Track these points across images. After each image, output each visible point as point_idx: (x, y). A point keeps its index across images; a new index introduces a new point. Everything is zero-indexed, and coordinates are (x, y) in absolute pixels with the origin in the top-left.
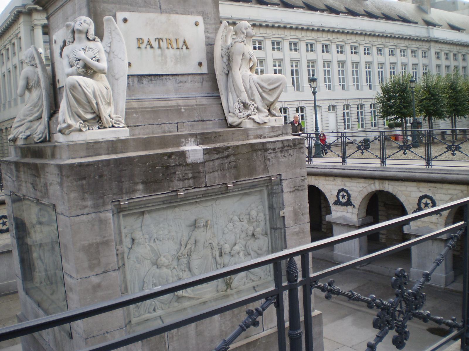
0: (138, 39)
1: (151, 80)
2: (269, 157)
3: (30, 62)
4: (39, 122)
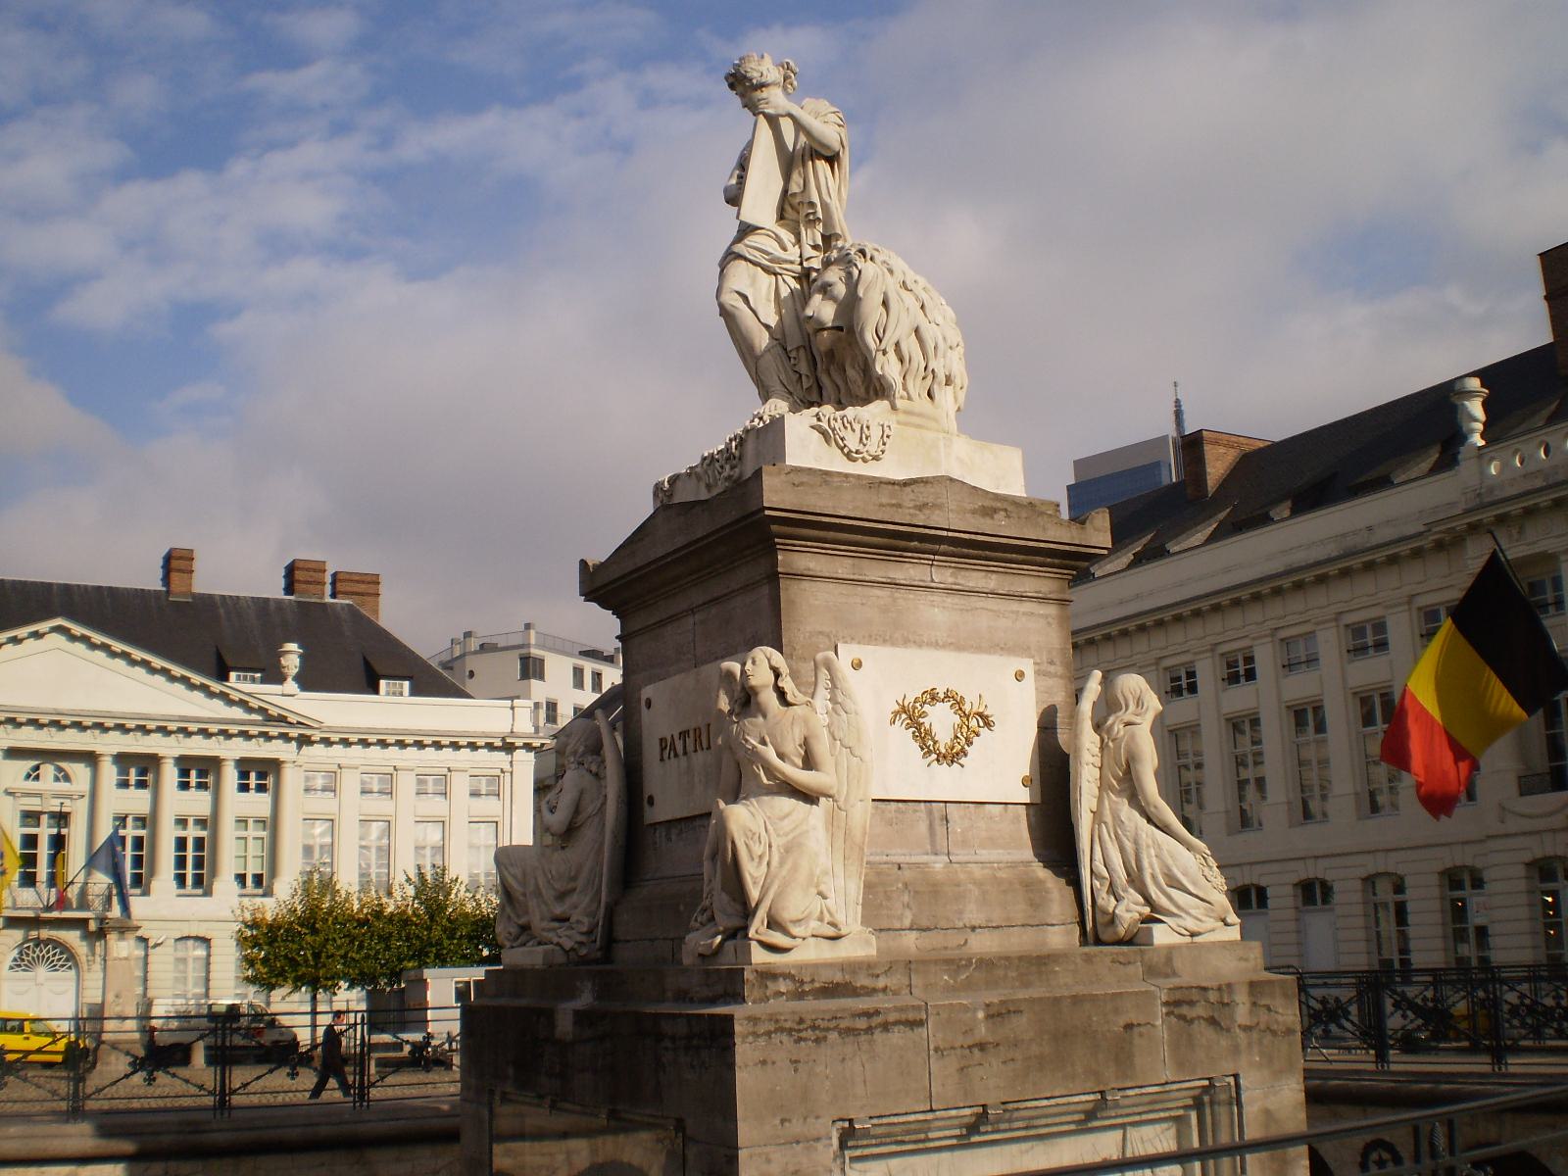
0: (661, 740)
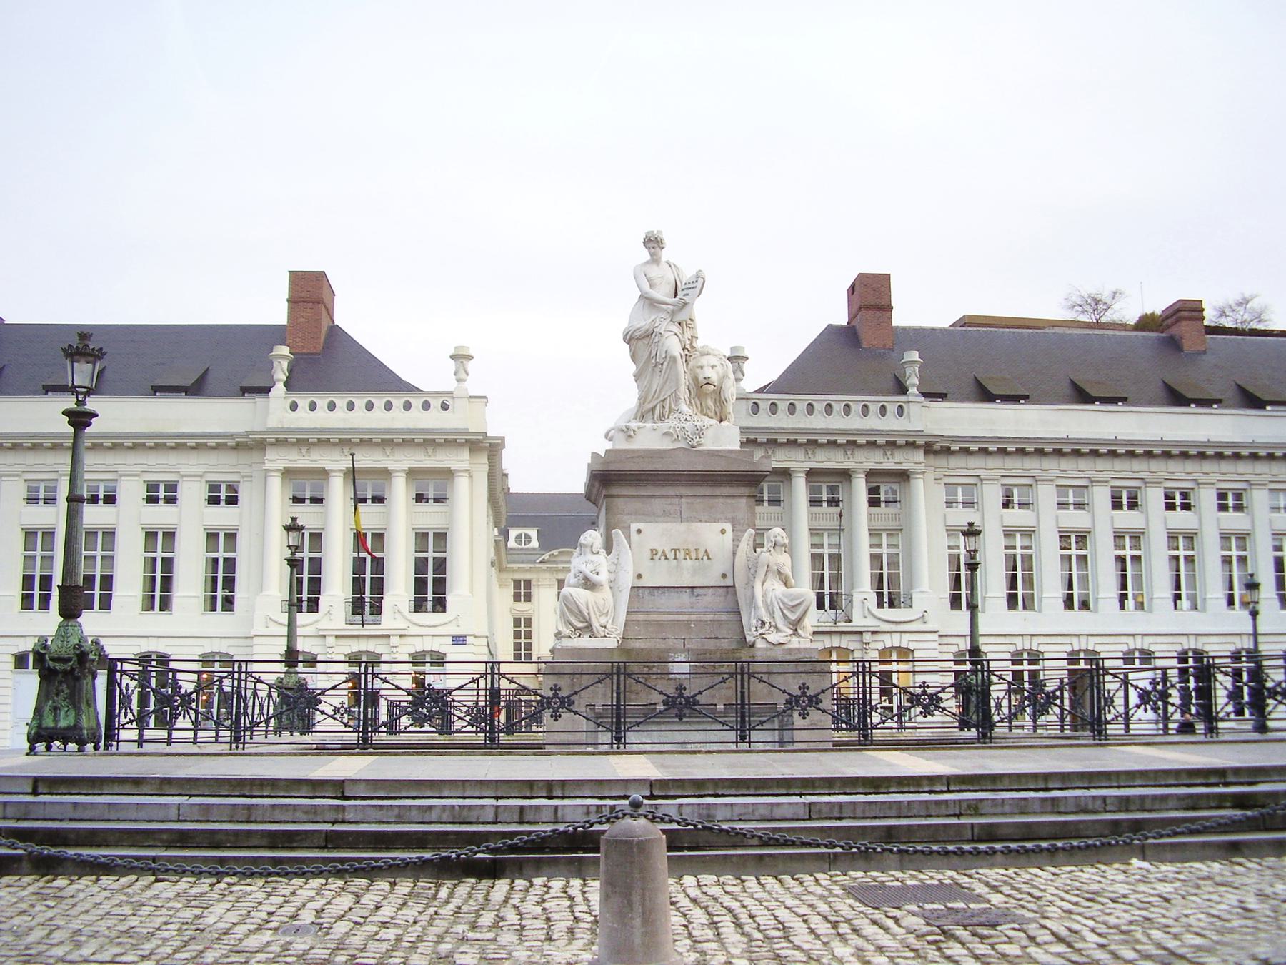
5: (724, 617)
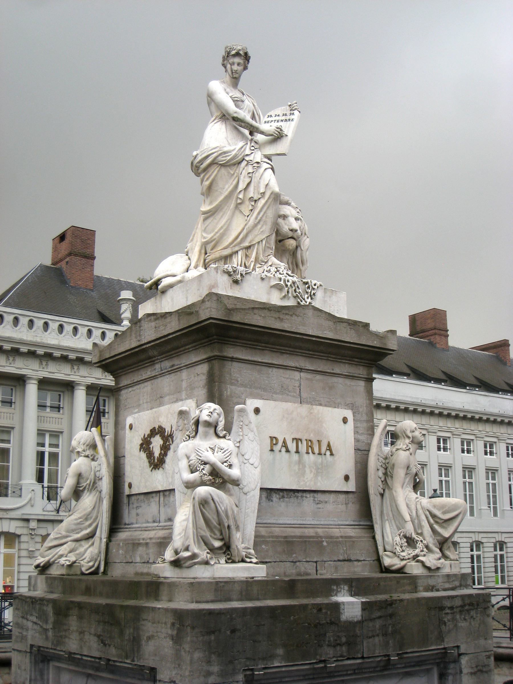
0: (272, 438)
1: (283, 497)
2: (446, 620)
3: (84, 451)
4: (90, 543)
5: (351, 532)
